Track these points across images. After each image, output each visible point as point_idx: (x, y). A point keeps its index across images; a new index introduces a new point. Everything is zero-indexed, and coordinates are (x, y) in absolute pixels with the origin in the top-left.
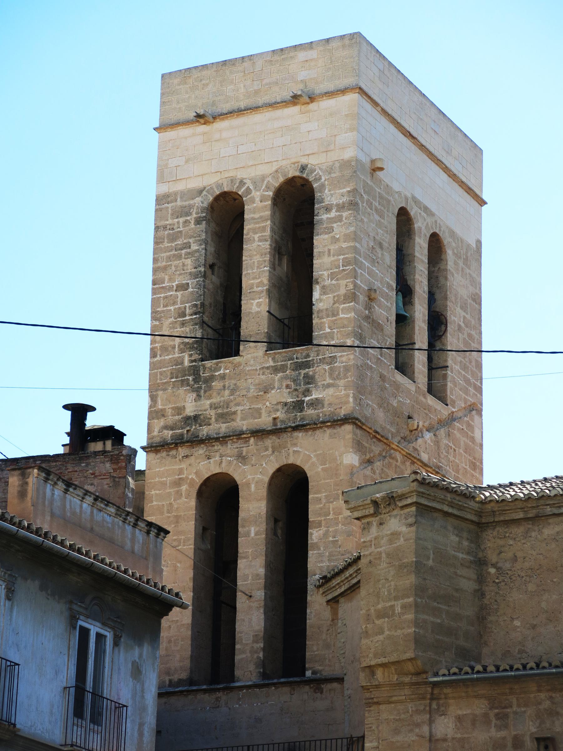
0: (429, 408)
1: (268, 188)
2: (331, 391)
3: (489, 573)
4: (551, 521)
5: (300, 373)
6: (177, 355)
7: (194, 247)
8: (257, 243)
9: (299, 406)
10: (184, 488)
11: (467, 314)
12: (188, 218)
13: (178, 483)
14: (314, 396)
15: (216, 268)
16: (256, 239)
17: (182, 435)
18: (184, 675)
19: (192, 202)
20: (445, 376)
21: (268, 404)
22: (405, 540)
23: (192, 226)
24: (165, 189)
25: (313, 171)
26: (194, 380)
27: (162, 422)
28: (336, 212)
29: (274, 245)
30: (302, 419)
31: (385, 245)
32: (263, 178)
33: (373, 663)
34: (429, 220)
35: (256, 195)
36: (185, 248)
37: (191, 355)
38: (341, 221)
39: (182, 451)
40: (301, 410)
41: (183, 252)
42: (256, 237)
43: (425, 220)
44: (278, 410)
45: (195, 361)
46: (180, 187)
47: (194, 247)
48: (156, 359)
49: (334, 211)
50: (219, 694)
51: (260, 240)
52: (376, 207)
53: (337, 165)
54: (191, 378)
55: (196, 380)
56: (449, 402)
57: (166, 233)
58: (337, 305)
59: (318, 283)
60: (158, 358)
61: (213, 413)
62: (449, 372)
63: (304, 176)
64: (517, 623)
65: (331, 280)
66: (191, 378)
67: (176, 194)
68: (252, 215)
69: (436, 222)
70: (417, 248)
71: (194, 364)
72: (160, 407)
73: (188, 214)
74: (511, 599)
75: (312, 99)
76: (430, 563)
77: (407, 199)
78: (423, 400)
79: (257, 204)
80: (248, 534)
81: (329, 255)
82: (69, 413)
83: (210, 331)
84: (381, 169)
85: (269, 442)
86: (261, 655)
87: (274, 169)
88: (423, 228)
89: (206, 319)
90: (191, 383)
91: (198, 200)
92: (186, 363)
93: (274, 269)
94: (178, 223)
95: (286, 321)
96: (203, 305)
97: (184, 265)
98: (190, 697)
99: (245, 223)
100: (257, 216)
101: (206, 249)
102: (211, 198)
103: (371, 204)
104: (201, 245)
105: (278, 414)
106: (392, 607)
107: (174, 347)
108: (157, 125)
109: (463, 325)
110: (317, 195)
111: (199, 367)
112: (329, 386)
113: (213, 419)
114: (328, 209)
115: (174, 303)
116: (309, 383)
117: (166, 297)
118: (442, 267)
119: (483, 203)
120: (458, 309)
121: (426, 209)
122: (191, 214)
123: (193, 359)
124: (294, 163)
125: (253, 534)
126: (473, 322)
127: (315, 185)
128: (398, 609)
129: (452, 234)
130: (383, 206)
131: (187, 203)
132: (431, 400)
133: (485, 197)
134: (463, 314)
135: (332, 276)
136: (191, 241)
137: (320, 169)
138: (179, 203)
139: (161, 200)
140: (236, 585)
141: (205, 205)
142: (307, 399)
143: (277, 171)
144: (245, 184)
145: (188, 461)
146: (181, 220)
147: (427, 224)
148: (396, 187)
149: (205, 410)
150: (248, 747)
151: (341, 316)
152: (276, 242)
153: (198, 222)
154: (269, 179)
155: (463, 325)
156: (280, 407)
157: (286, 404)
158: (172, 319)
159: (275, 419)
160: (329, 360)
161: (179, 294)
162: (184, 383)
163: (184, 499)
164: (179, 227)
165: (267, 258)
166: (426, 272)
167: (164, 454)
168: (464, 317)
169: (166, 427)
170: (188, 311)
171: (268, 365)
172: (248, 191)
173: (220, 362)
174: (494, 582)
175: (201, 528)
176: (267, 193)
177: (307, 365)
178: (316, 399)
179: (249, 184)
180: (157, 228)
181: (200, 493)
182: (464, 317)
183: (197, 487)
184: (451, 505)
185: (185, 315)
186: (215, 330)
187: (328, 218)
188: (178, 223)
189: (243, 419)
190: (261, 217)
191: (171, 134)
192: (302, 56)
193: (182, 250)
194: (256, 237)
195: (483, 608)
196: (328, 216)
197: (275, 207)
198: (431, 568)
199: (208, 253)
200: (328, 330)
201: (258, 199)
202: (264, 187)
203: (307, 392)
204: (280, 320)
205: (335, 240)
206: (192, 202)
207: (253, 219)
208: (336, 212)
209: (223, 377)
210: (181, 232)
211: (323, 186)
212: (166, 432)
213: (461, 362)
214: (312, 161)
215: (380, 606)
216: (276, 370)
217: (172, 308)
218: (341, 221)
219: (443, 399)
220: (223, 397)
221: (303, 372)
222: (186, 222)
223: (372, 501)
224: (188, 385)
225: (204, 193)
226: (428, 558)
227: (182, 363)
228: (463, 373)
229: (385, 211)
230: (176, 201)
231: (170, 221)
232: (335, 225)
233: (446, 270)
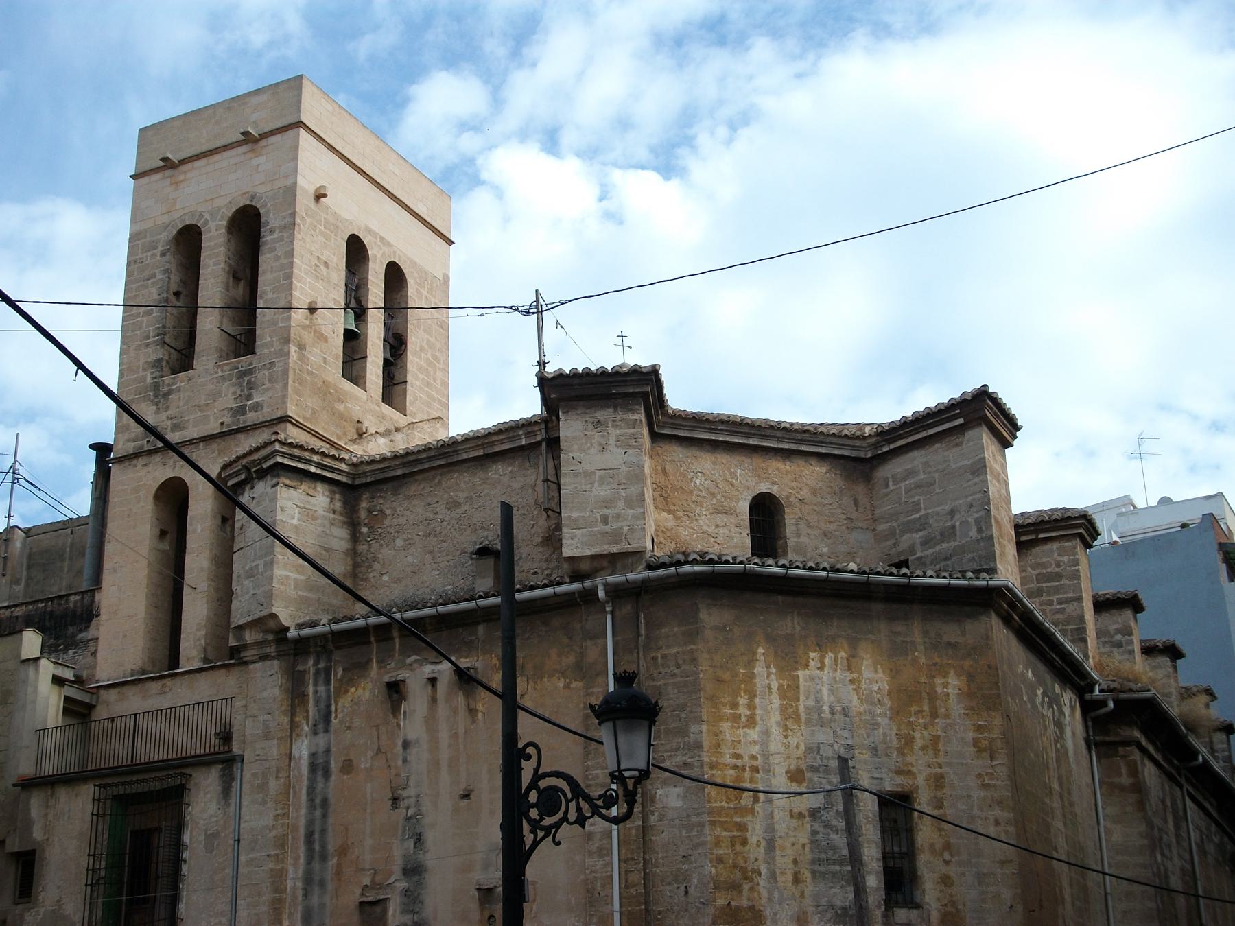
0: (383, 417)
1: (222, 217)
2: (270, 394)
3: (361, 533)
4: (417, 477)
5: (244, 380)
6: (141, 373)
7: (159, 276)
8: (210, 270)
9: (242, 410)
10: (142, 493)
11: (431, 337)
12: (155, 251)
13: (137, 490)
14: (255, 400)
15: (182, 296)
16: (211, 264)
17: (142, 446)
18: (136, 668)
19: (159, 237)
20: (405, 391)
21: (215, 410)
22: (270, 501)
23: (158, 258)
24: (137, 228)
25: (260, 198)
26: (154, 394)
27: (126, 436)
28: (279, 232)
29: (227, 269)
30: (244, 422)
31: (332, 265)
32: (219, 208)
33: (240, 623)
34: (386, 249)
35: (212, 225)
36: (152, 278)
37: (152, 373)
38: (282, 240)
39: (141, 461)
40: (244, 414)
41: (150, 282)
42: (211, 262)
43: (381, 249)
44: (224, 416)
45: (156, 378)
46: (150, 224)
48: (123, 379)
49: (277, 232)
50: (164, 681)
51: (215, 265)
52: (321, 230)
53: (281, 191)
54: (151, 394)
55: (156, 396)
56: (408, 413)
57: (136, 266)
58: (277, 316)
59: (261, 298)
60: (125, 378)
61: (169, 423)
62: (409, 387)
63: (253, 204)
64: (386, 578)
65: (273, 293)
66: (151, 394)
67: (146, 231)
68: (208, 244)
69: (395, 252)
70: (371, 273)
71: (155, 380)
72: (125, 422)
73: (155, 248)
74: (380, 556)
75: (263, 136)
76: (295, 522)
77: (360, 229)
78: (377, 408)
79: (213, 233)
80: (195, 531)
81: (272, 272)
82: (94, 452)
83: (173, 351)
84: (325, 196)
85: (215, 445)
86: (203, 642)
87: (228, 201)
88: (379, 256)
89: (167, 339)
90: (152, 398)
91: (165, 234)
92: (149, 380)
93: (228, 290)
94: (147, 256)
95: (238, 337)
96: (164, 327)
97: (150, 293)
98: (140, 685)
99: (202, 251)
100: (212, 243)
101: (169, 278)
102: (175, 232)
103: (315, 226)
104: (164, 274)
105: (224, 419)
106: (257, 565)
107: (138, 368)
108: (133, 173)
109: (426, 347)
110: (264, 219)
111: (159, 382)
112: (268, 389)
113: (169, 428)
114: (272, 231)
115: (140, 328)
116: (251, 388)
117: (134, 323)
118: (403, 294)
119: (451, 242)
120: (421, 331)
121: (382, 239)
122: (157, 248)
123: (154, 376)
124: (245, 194)
125: (199, 531)
126: (438, 346)
127: (262, 211)
128: (261, 568)
129: (414, 264)
130: (329, 229)
131: (154, 238)
132: (386, 409)
133: (452, 239)
134: (426, 336)
135: (274, 290)
136: (157, 271)
137: (266, 197)
138: (148, 239)
139: (134, 237)
140: (183, 579)
141: (170, 238)
142: (250, 402)
143: (230, 202)
144: (203, 216)
145: (146, 469)
146: (149, 254)
147: (384, 252)
148: (345, 215)
149: (163, 421)
150: (136, 715)
151: (281, 325)
152: (230, 266)
153: (163, 255)
154: (224, 210)
155: (426, 347)
156: (226, 412)
157: (231, 409)
158: (139, 343)
159: (222, 424)
160: (268, 366)
161: (145, 319)
162: (145, 399)
163: (142, 504)
164: (147, 260)
166: (383, 296)
167: (127, 464)
168: (428, 341)
169: (129, 440)
170: (151, 334)
171: (217, 375)
172: (206, 222)
173: (178, 377)
174: (366, 540)
175: (158, 530)
176: (221, 223)
177: (250, 372)
178: (257, 402)
179: (207, 216)
180: (129, 264)
181: (157, 497)
182: (428, 341)
183: (153, 491)
184: (319, 465)
185: (148, 338)
186: (179, 351)
187: (271, 239)
188: (147, 256)
189: (194, 426)
190: (216, 244)
191: (145, 180)
192: (255, 100)
193: (148, 280)
194: (211, 262)
195: (356, 565)
196: (272, 237)
197: (230, 236)
198: (296, 527)
199: (172, 281)
200: (269, 339)
201: (213, 229)
202: (219, 217)
203: (249, 397)
204: (233, 337)
205: (277, 258)
206: (159, 237)
207: (209, 246)
208: (279, 232)
209: (178, 390)
210: (148, 265)
211: (268, 212)
212: (128, 444)
213: (423, 379)
214: (260, 190)
215: (247, 568)
216: (223, 378)
217: (138, 332)
218: (282, 240)
219: (403, 411)
220: (178, 407)
221: (246, 379)
222: (152, 255)
223: (243, 466)
224: (149, 400)
225: (170, 228)
226: (293, 518)
227: (145, 381)
228: (426, 389)
229: (333, 235)
230: (146, 236)
231: (140, 256)
232: (277, 245)
233: (407, 296)
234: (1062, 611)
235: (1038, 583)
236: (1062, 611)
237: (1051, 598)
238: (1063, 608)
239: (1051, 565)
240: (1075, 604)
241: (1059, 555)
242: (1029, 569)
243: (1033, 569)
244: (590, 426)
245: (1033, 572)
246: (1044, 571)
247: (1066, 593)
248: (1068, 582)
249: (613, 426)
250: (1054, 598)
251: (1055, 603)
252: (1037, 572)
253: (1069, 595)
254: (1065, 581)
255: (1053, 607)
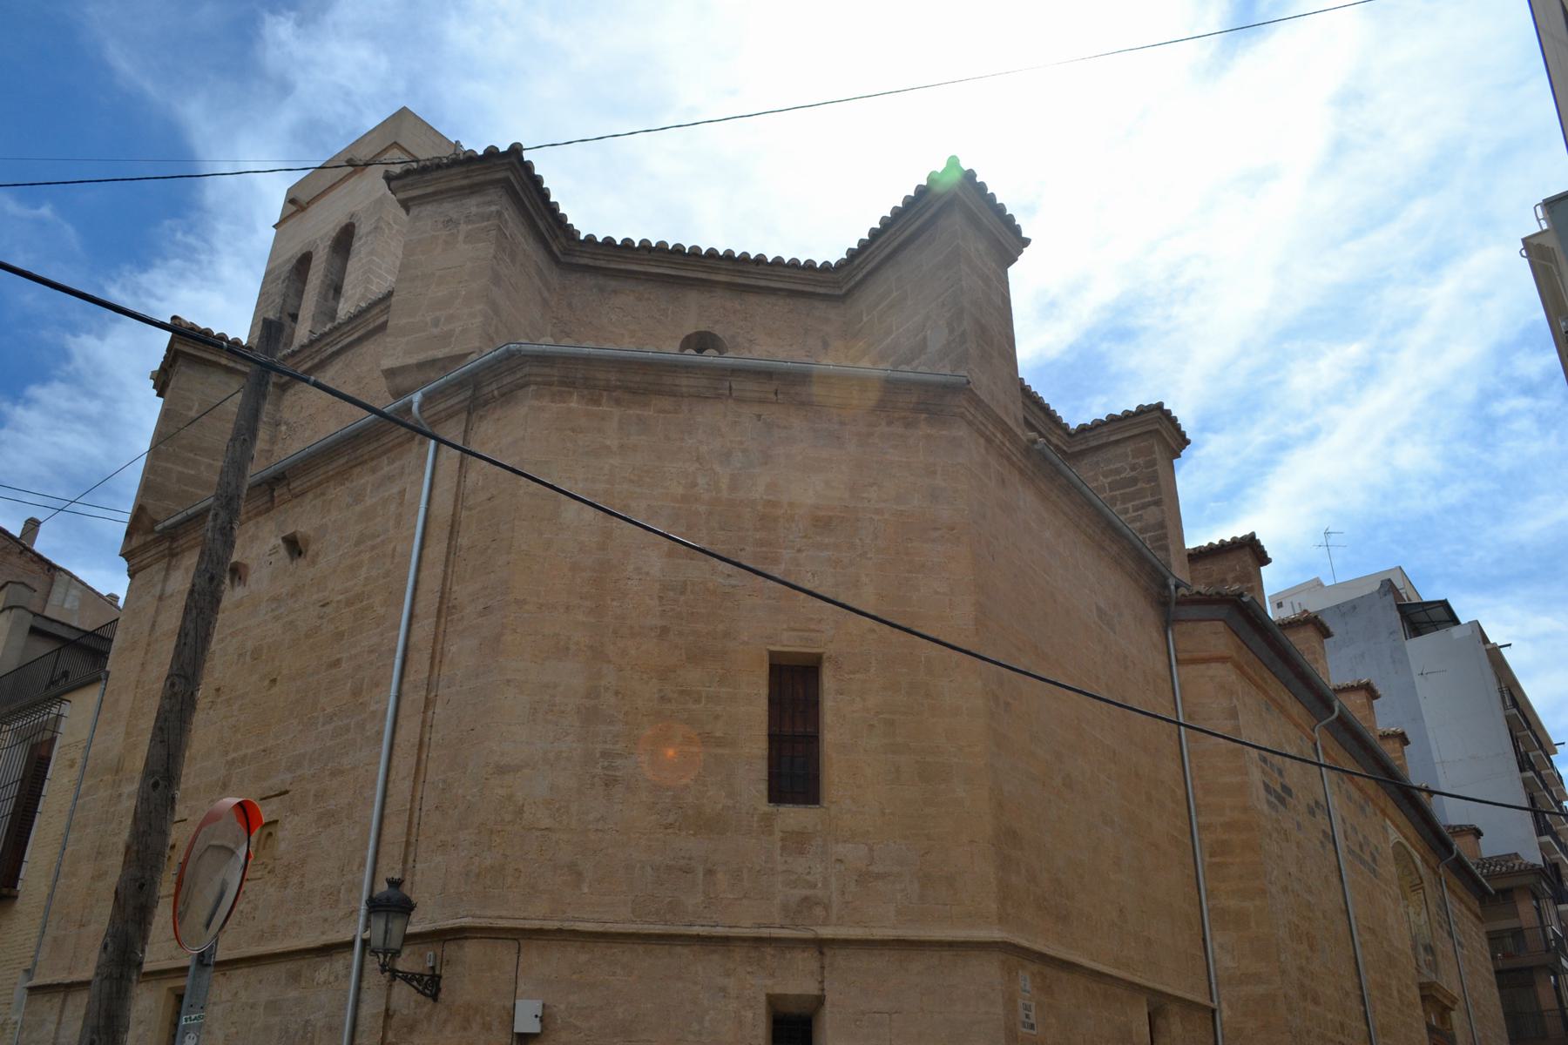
1: (329, 239)
35: (321, 247)
47: (277, 301)
93: (326, 300)
165: (317, 291)
234: (1139, 518)
235: (1110, 492)
236: (1139, 518)
237: (1126, 506)
238: (1141, 515)
239: (1126, 469)
240: (1153, 508)
241: (1133, 458)
242: (1101, 478)
243: (1106, 476)
244: (440, 226)
245: (1104, 480)
246: (1118, 478)
247: (1144, 497)
248: (1144, 485)
249: (465, 222)
250: (1130, 505)
251: (1131, 510)
252: (1109, 480)
253: (1146, 500)
254: (1139, 485)
255: (1129, 515)
